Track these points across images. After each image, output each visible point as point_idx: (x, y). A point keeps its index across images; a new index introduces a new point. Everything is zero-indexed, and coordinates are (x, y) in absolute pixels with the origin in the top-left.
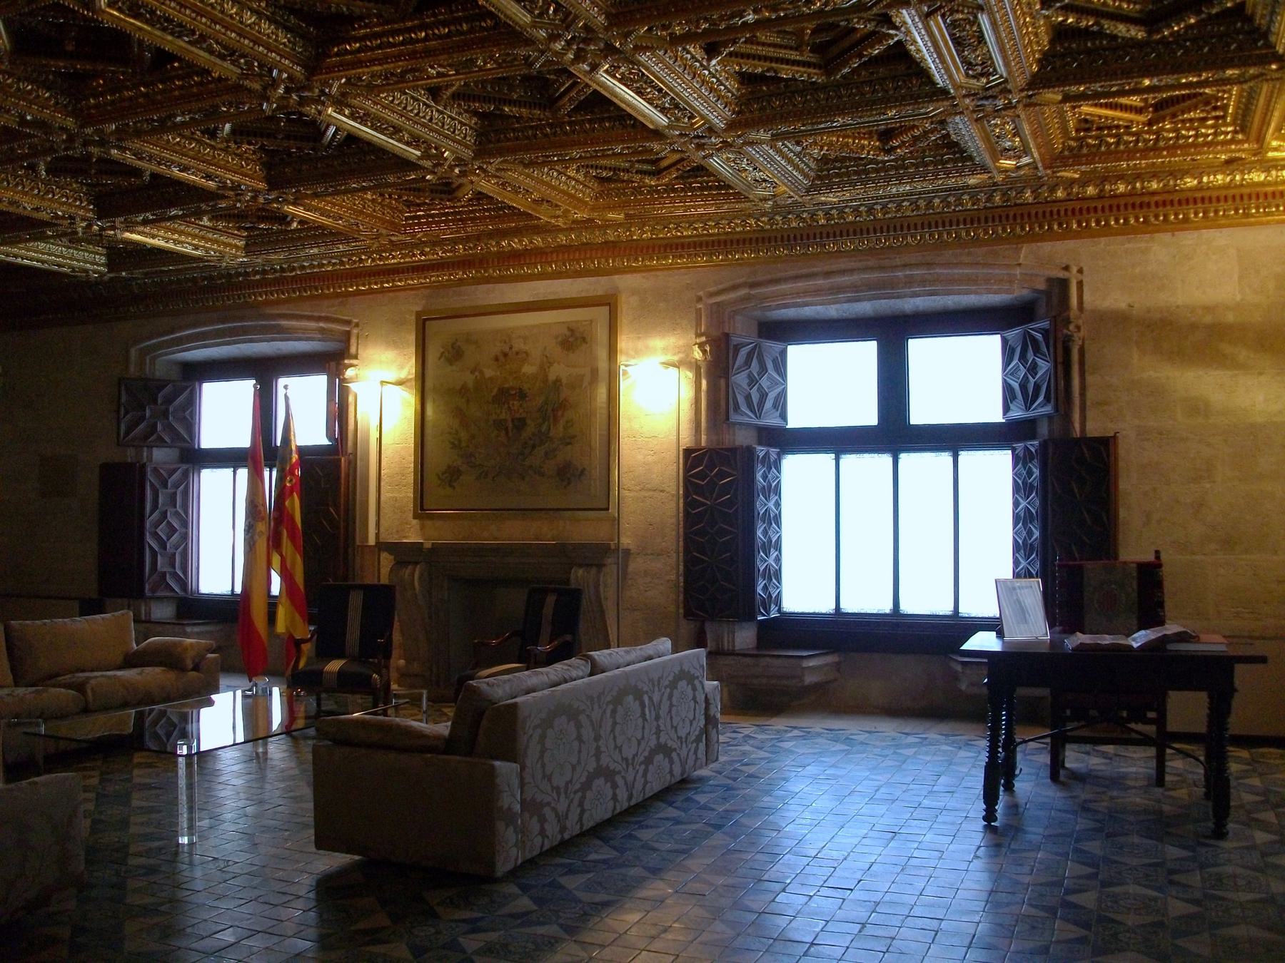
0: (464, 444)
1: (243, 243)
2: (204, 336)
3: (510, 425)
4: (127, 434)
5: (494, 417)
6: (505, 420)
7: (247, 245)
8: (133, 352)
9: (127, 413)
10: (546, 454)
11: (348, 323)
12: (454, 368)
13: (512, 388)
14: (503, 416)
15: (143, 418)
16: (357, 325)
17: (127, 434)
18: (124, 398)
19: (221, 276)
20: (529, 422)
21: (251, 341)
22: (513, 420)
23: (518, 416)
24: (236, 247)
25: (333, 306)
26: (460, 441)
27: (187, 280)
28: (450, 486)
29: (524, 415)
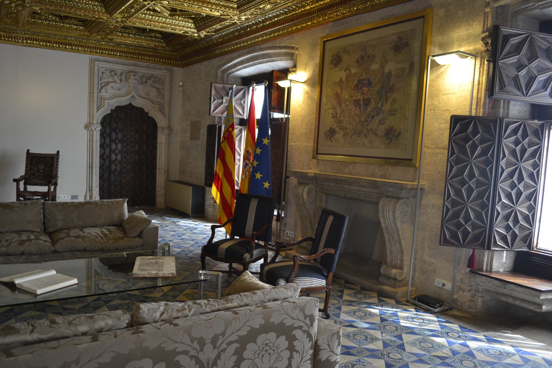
0: (338, 115)
1: (235, 6)
2: (242, 63)
3: (362, 103)
4: (214, 111)
5: (354, 98)
6: (360, 100)
7: (238, 7)
8: (219, 72)
9: (214, 100)
10: (380, 121)
11: (293, 48)
12: (337, 69)
13: (365, 79)
14: (359, 97)
15: (222, 102)
16: (297, 49)
17: (214, 111)
18: (213, 93)
19: (242, 29)
20: (372, 101)
21: (260, 63)
22: (364, 100)
23: (366, 97)
24: (232, 8)
25: (288, 39)
26: (336, 114)
27: (231, 33)
28: (331, 140)
29: (369, 96)
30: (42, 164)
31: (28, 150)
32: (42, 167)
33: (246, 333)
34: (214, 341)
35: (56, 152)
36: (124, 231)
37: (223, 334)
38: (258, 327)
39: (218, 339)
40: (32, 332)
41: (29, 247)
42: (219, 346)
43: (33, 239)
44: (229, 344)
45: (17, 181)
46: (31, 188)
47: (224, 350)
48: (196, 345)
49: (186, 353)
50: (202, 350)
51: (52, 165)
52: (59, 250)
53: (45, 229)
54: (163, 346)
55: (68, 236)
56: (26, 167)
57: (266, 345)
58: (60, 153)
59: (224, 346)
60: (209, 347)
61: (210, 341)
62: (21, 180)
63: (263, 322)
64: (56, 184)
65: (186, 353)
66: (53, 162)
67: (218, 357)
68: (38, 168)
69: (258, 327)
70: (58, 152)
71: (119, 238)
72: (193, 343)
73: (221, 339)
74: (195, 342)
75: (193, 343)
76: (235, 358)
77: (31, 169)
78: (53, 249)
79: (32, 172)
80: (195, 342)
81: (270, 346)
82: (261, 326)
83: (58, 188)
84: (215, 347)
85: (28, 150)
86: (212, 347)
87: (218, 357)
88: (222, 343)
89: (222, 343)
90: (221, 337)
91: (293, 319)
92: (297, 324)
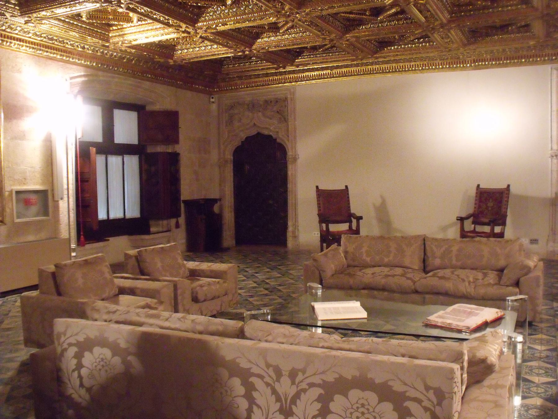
30: (491, 200)
31: (478, 186)
32: (490, 204)
33: (334, 380)
34: (293, 375)
35: (505, 187)
36: (500, 278)
37: (304, 371)
38: (350, 378)
39: (297, 375)
40: (167, 320)
41: (393, 282)
42: (299, 383)
43: (398, 275)
44: (312, 385)
45: (461, 220)
46: (479, 228)
47: (304, 391)
48: (271, 372)
49: (261, 377)
50: (278, 380)
51: (500, 202)
52: (419, 290)
53: (424, 268)
54: (237, 360)
55: (434, 276)
56: (476, 204)
57: (363, 405)
58: (511, 188)
59: (304, 386)
60: (286, 380)
61: (287, 373)
62: (467, 218)
63: (357, 374)
64: (504, 224)
65: (261, 377)
66: (502, 198)
67: (297, 396)
68: (486, 204)
69: (350, 378)
70: (509, 186)
71: (489, 284)
72: (268, 369)
73: (300, 377)
74: (271, 369)
75: (268, 369)
76: (318, 406)
77: (480, 207)
78: (413, 287)
79: (481, 210)
80: (271, 369)
81: (368, 409)
82: (354, 378)
83: (506, 227)
84: (293, 383)
85: (478, 186)
86: (289, 382)
87: (297, 396)
88: (302, 381)
89: (302, 381)
90: (300, 374)
91: (405, 384)
92: (412, 393)
